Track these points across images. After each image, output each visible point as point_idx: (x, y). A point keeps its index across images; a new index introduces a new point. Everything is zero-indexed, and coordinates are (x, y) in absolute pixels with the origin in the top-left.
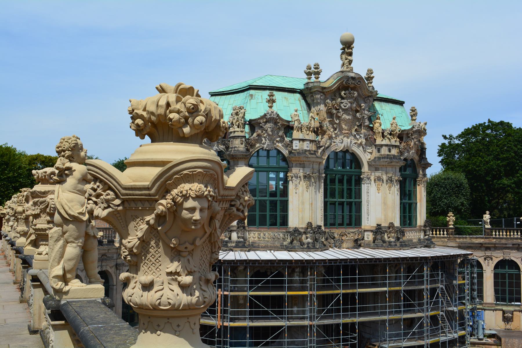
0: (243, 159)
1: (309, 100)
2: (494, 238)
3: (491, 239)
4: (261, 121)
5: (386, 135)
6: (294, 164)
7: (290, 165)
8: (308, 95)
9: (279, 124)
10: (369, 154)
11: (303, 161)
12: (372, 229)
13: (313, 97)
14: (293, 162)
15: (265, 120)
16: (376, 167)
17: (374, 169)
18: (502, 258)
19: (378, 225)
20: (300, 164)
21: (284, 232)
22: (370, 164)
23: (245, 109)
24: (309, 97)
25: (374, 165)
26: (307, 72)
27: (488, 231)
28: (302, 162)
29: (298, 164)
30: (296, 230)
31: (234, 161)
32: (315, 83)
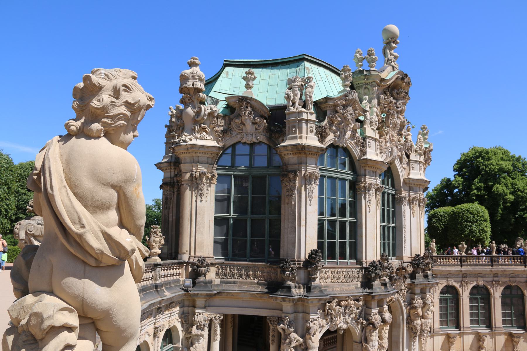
0: (315, 156)
1: (363, 91)
2: (440, 265)
3: (438, 266)
4: (339, 102)
5: (418, 150)
6: (367, 171)
7: (363, 172)
8: (362, 86)
9: (357, 112)
10: (404, 170)
11: (378, 168)
12: (410, 260)
13: (367, 89)
14: (367, 168)
15: (344, 103)
16: (411, 186)
17: (408, 188)
18: (445, 284)
19: (417, 256)
20: (373, 172)
21: (358, 268)
22: (406, 182)
23: (314, 83)
24: (363, 88)
25: (409, 184)
26: (358, 57)
27: (435, 259)
28: (375, 170)
29: (371, 172)
30: (373, 264)
31: (298, 157)
32: (373, 71)
